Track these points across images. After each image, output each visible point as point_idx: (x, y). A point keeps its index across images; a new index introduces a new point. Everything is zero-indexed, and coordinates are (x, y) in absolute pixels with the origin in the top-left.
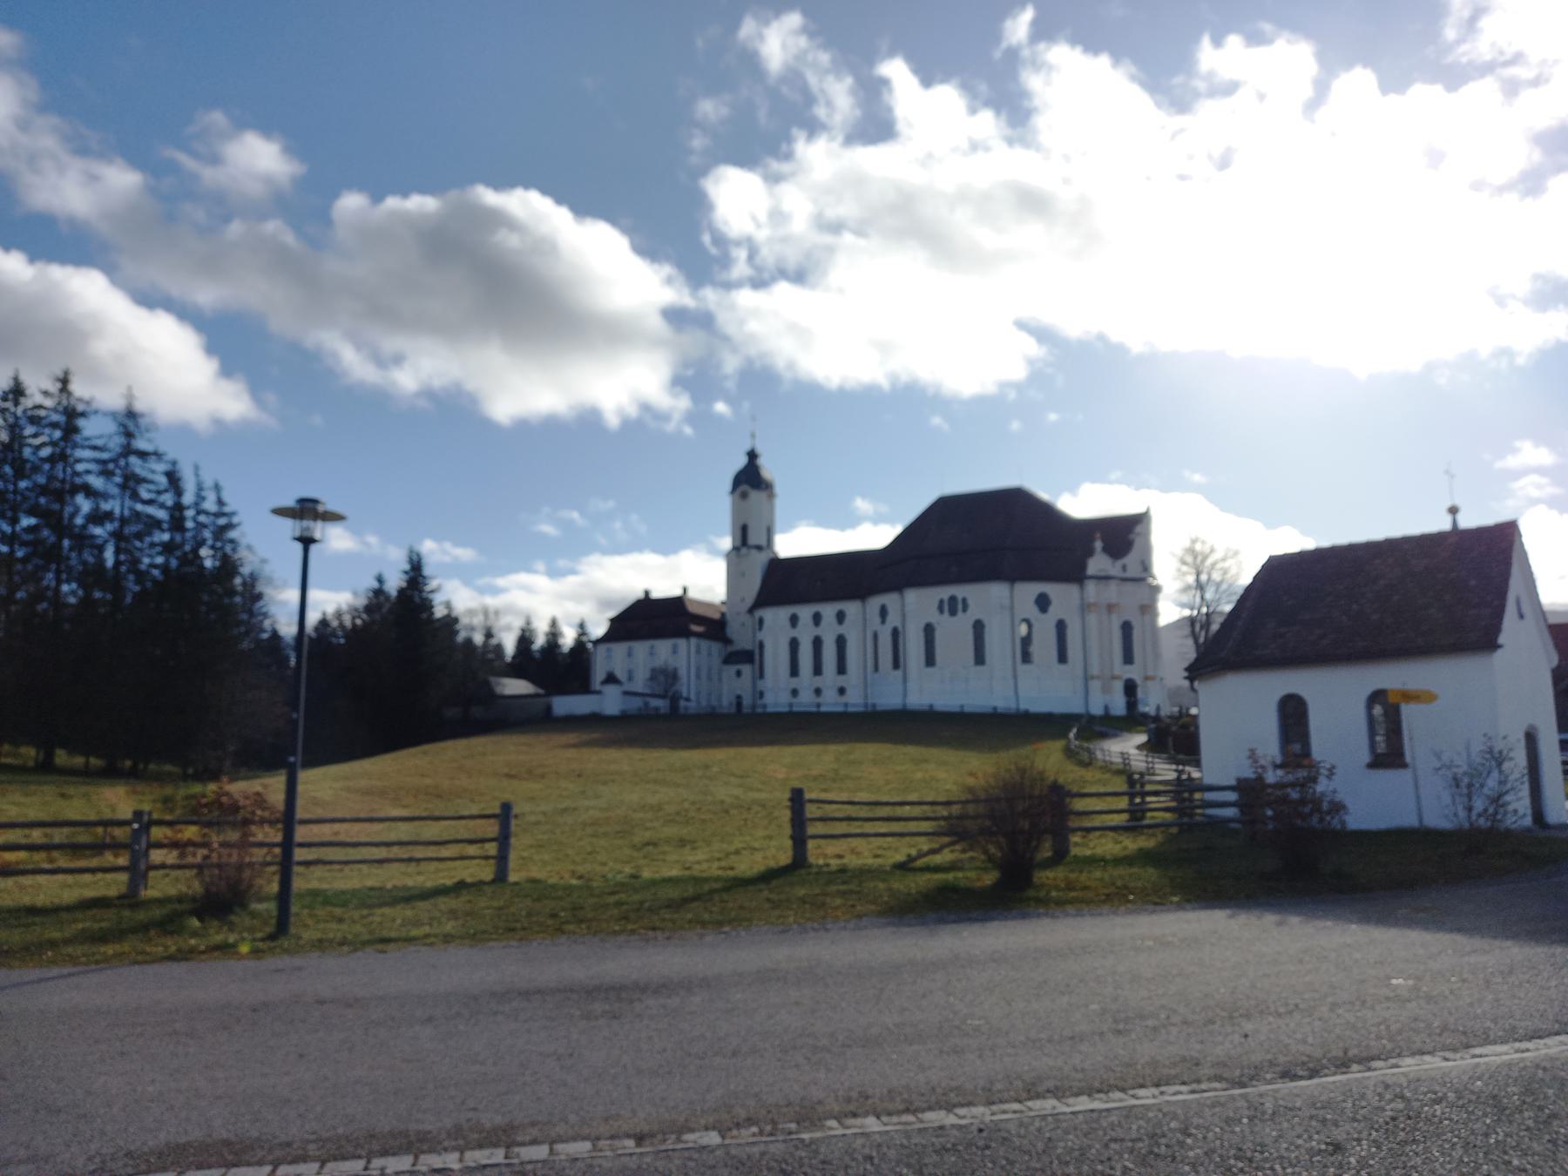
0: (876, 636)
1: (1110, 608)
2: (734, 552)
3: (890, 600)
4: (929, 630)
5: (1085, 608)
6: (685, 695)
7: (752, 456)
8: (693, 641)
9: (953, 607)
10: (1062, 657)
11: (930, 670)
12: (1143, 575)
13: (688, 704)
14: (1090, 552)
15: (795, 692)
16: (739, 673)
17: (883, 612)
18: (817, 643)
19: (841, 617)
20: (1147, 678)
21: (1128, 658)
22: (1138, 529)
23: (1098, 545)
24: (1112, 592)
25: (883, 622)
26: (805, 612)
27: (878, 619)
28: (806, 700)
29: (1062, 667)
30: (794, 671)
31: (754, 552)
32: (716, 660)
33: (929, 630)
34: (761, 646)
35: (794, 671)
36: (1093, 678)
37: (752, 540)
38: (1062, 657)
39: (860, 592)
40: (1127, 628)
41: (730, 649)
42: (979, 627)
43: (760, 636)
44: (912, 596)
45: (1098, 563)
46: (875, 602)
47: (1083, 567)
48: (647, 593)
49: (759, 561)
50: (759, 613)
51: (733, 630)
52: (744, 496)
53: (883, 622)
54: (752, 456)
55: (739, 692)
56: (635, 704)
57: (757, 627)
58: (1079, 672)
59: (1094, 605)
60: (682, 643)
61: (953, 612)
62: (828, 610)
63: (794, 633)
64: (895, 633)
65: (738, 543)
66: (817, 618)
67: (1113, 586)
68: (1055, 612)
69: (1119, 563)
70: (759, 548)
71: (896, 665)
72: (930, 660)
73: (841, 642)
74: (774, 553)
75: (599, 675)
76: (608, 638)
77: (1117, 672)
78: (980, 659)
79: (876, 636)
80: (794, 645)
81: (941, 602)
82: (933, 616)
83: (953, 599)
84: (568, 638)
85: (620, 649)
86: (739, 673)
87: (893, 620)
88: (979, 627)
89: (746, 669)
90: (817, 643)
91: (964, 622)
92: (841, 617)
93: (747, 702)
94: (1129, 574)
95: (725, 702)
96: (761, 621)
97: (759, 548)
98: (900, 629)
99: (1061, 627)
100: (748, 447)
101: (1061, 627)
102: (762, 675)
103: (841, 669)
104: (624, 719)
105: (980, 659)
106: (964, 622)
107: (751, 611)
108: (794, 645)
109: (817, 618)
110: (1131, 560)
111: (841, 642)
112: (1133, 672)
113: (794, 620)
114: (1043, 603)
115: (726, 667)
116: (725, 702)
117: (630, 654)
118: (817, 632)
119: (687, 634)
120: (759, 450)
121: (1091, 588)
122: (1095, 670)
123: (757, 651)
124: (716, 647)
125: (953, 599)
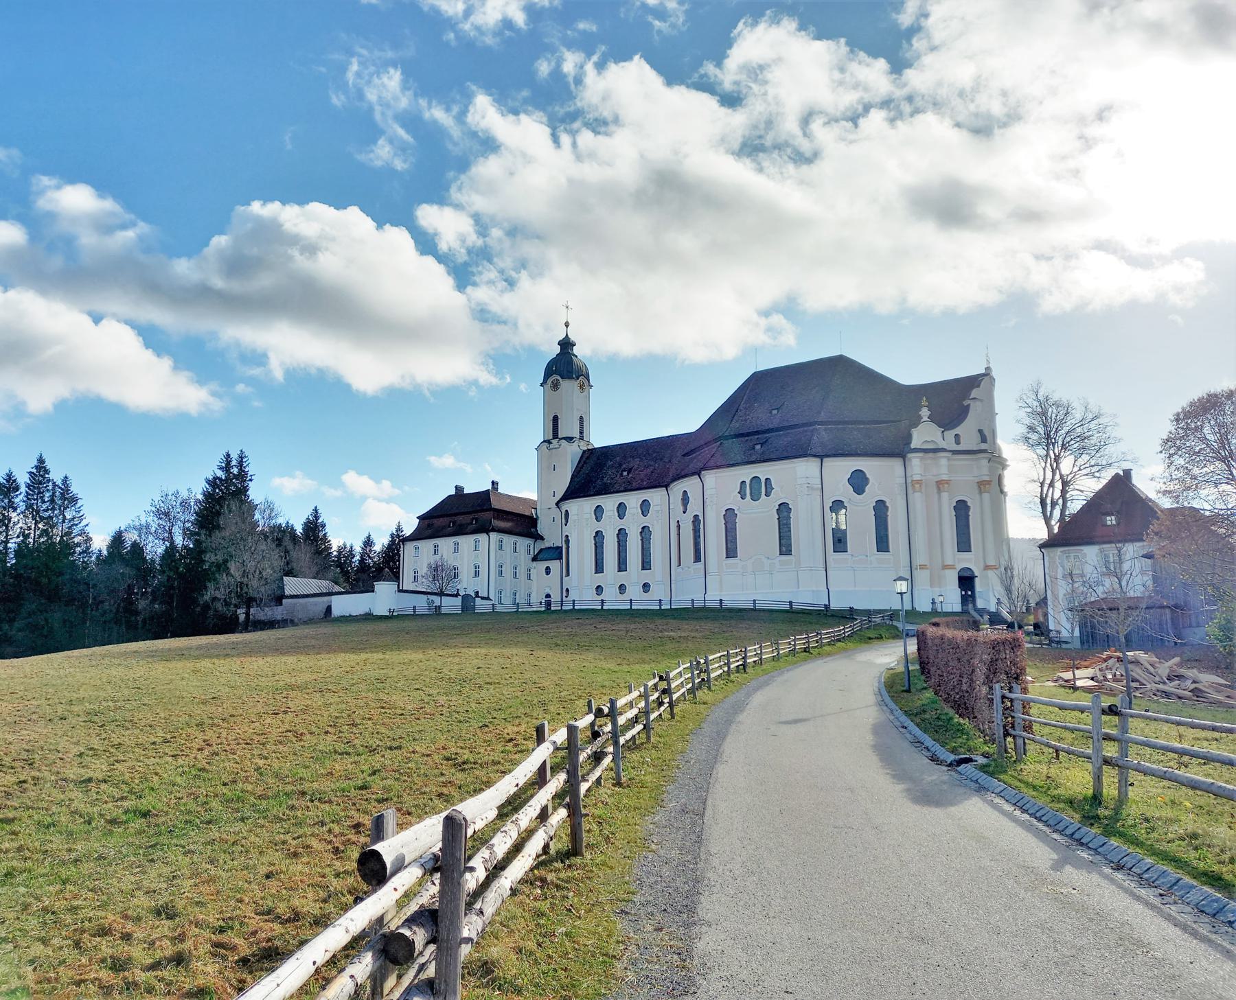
0: (679, 527)
4: (730, 516)
7: (566, 345)
8: (493, 535)
9: (756, 489)
10: (882, 544)
11: (731, 561)
14: (916, 422)
15: (599, 589)
16: (548, 571)
17: (685, 499)
18: (622, 535)
19: (645, 507)
21: (964, 544)
22: (974, 393)
23: (925, 413)
24: (942, 467)
26: (609, 503)
27: (681, 509)
28: (613, 599)
29: (883, 555)
30: (599, 568)
31: (564, 442)
32: (524, 559)
33: (730, 516)
34: (567, 541)
35: (599, 568)
38: (882, 544)
39: (661, 482)
40: (962, 509)
41: (541, 545)
42: (784, 510)
44: (710, 477)
45: (924, 434)
46: (678, 488)
47: (908, 438)
48: (459, 489)
49: (569, 457)
50: (567, 505)
51: (542, 528)
52: (555, 386)
54: (566, 345)
55: (548, 591)
59: (918, 482)
61: (755, 497)
62: (633, 500)
63: (598, 526)
66: (621, 510)
67: (943, 461)
68: (873, 492)
69: (950, 435)
70: (569, 439)
71: (697, 558)
72: (731, 552)
74: (588, 443)
77: (949, 562)
78: (785, 548)
79: (679, 527)
82: (733, 501)
83: (755, 479)
85: (426, 546)
86: (548, 571)
87: (694, 508)
88: (784, 510)
89: (555, 565)
90: (622, 535)
92: (645, 507)
93: (556, 598)
95: (535, 599)
97: (569, 439)
98: (701, 518)
99: (881, 509)
101: (881, 509)
102: (568, 574)
103: (646, 565)
105: (785, 548)
106: (766, 508)
107: (557, 504)
109: (621, 510)
110: (967, 431)
113: (599, 512)
114: (858, 482)
116: (535, 599)
120: (572, 337)
121: (915, 461)
124: (523, 543)
125: (755, 479)
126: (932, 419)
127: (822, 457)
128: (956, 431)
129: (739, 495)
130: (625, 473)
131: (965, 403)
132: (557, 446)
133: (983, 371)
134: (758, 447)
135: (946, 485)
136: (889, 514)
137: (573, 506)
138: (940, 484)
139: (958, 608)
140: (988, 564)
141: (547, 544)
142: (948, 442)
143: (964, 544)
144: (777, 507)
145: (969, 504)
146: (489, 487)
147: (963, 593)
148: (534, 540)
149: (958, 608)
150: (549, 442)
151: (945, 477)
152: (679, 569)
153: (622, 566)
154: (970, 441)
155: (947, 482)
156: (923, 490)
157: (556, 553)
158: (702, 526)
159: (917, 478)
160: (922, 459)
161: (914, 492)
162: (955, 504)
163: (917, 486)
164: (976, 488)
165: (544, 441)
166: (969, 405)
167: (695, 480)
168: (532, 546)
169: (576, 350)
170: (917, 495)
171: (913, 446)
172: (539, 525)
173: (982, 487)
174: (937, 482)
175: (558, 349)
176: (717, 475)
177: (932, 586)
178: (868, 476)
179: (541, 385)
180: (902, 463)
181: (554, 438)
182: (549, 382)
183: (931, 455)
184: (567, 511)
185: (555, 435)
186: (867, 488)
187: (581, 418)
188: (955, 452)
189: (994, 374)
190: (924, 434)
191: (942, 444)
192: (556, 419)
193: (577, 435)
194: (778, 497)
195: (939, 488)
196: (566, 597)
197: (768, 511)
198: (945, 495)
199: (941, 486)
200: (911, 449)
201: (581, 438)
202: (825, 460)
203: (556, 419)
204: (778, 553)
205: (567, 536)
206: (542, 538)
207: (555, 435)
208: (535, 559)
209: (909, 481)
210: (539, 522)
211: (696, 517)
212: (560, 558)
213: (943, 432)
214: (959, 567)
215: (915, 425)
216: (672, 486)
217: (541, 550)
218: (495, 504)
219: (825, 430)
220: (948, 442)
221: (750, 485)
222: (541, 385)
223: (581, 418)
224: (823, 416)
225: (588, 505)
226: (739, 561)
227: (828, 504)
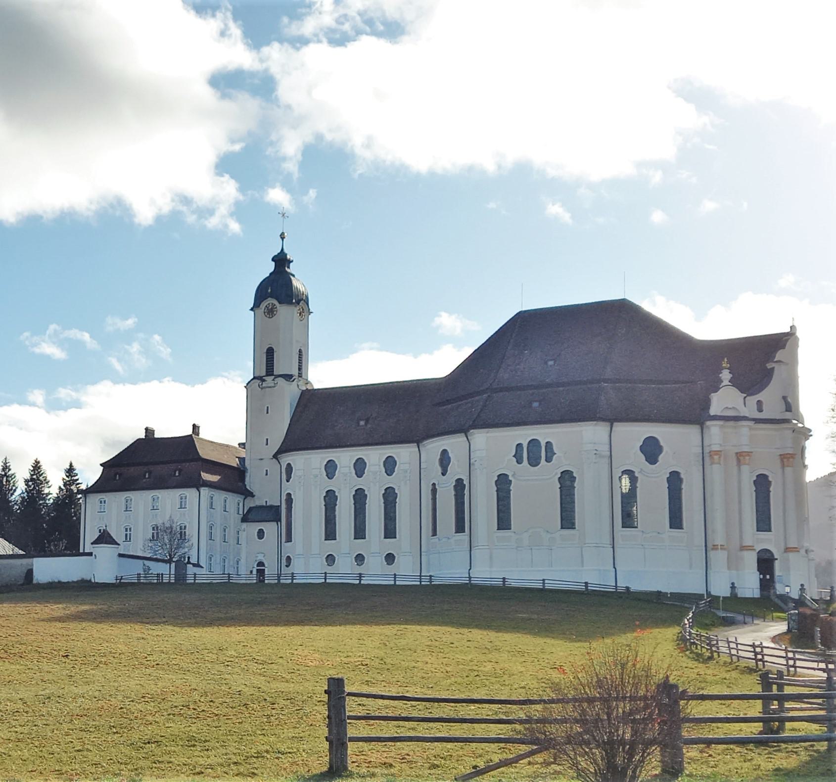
0: (434, 491)
1: (740, 457)
3: (453, 444)
4: (503, 482)
5: (706, 457)
6: (194, 560)
7: (281, 261)
12: (788, 415)
13: (197, 570)
16: (261, 534)
17: (444, 460)
18: (360, 497)
19: (390, 465)
20: (787, 550)
21: (764, 523)
22: (779, 356)
24: (744, 435)
25: (443, 474)
26: (345, 458)
27: (439, 470)
30: (330, 534)
31: (280, 381)
33: (503, 482)
34: (289, 499)
35: (330, 534)
36: (715, 547)
37: (280, 368)
40: (762, 484)
41: (251, 503)
42: (567, 480)
43: (288, 488)
44: (481, 438)
46: (434, 447)
50: (287, 459)
51: (252, 481)
53: (443, 474)
54: (281, 261)
56: (132, 571)
59: (717, 453)
60: (190, 494)
61: (534, 461)
62: (374, 456)
63: (331, 485)
64: (459, 486)
66: (360, 467)
67: (745, 428)
70: (288, 377)
71: (460, 528)
73: (390, 497)
75: (89, 533)
76: (99, 487)
79: (434, 491)
80: (330, 499)
81: (519, 446)
84: (54, 486)
86: (261, 534)
87: (457, 470)
88: (567, 480)
90: (360, 497)
92: (390, 465)
93: (270, 571)
95: (243, 571)
96: (289, 469)
97: (288, 377)
98: (466, 482)
99: (675, 481)
101: (675, 481)
102: (289, 539)
103: (390, 532)
104: (119, 587)
107: (275, 456)
108: (330, 499)
109: (360, 467)
111: (390, 497)
112: (769, 541)
113: (331, 468)
115: (244, 525)
116: (243, 571)
118: (360, 483)
119: (198, 484)
121: (714, 429)
122: (719, 538)
123: (284, 506)
125: (534, 443)
126: (734, 382)
129: (515, 459)
130: (362, 423)
132: (273, 385)
134: (535, 404)
135: (747, 458)
136: (683, 486)
137: (298, 460)
138: (739, 456)
139: (757, 594)
140: (789, 546)
141: (259, 501)
142: (747, 407)
143: (764, 523)
145: (770, 479)
147: (762, 576)
148: (243, 497)
149: (757, 594)
150: (261, 379)
151: (746, 449)
152: (435, 540)
153: (360, 532)
154: (773, 409)
155: (749, 454)
156: (722, 462)
157: (271, 513)
158: (466, 492)
159: (715, 448)
160: (721, 427)
161: (712, 463)
162: (755, 478)
163: (716, 457)
164: (779, 461)
165: (254, 378)
166: (773, 368)
168: (241, 504)
169: (292, 269)
170: (715, 466)
171: (713, 411)
172: (247, 479)
173: (785, 460)
174: (737, 453)
175: (271, 267)
176: (488, 435)
177: (729, 568)
178: (662, 443)
180: (700, 430)
181: (267, 375)
182: (263, 305)
184: (289, 465)
185: (270, 371)
186: (660, 458)
187: (300, 351)
189: (799, 334)
191: (744, 412)
192: (270, 352)
193: (295, 372)
195: (739, 461)
196: (287, 566)
197: (551, 478)
198: (745, 469)
199: (741, 458)
200: (710, 416)
201: (300, 375)
202: (615, 424)
203: (270, 352)
204: (560, 527)
205: (289, 495)
206: (251, 495)
207: (270, 371)
208: (245, 519)
209: (707, 450)
210: (248, 475)
211: (459, 482)
212: (278, 520)
213: (745, 398)
214: (758, 548)
215: (716, 389)
217: (251, 509)
218: (204, 453)
220: (749, 410)
221: (528, 448)
222: (252, 309)
223: (300, 351)
224: (609, 373)
225: (316, 460)
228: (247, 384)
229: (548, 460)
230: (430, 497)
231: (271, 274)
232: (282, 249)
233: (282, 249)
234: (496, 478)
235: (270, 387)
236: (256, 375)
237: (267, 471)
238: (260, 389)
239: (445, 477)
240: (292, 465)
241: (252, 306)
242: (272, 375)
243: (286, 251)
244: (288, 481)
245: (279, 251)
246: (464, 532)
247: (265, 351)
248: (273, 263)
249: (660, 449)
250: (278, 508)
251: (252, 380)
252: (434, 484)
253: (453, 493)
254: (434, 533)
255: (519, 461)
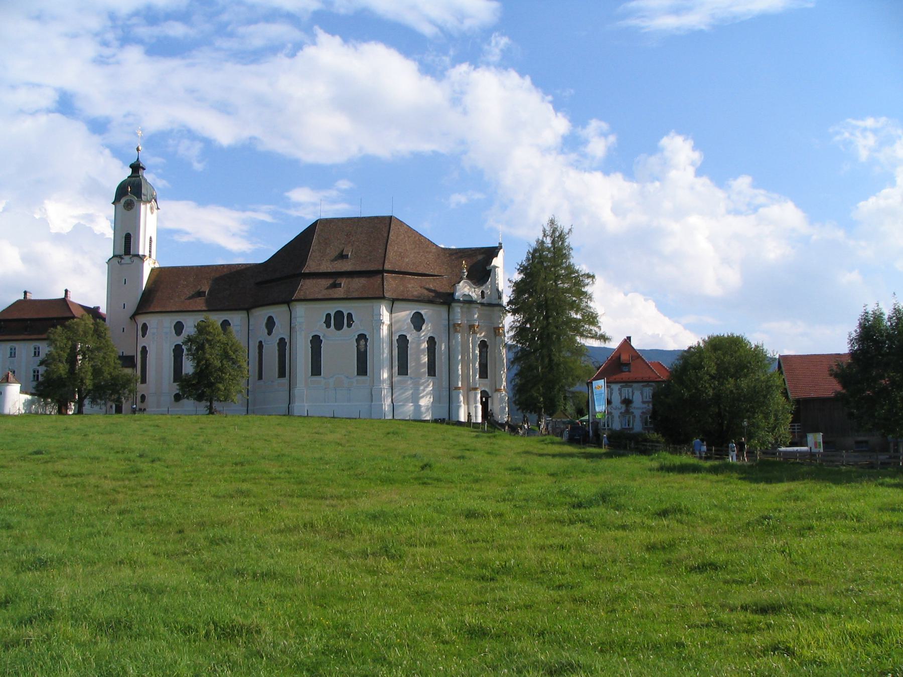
2: (116, 260)
3: (278, 312)
4: (316, 342)
5: (452, 328)
9: (339, 321)
17: (270, 324)
25: (270, 333)
27: (266, 331)
31: (136, 259)
33: (316, 342)
34: (144, 349)
43: (142, 342)
44: (300, 310)
46: (261, 315)
50: (141, 320)
52: (129, 206)
53: (270, 333)
57: (140, 333)
58: (445, 384)
61: (338, 326)
65: (121, 251)
68: (427, 330)
71: (282, 374)
72: (316, 370)
78: (362, 369)
81: (328, 315)
82: (320, 329)
83: (339, 314)
87: (280, 330)
91: (348, 336)
94: (485, 301)
96: (145, 328)
99: (432, 341)
100: (134, 160)
102: (144, 381)
105: (362, 369)
106: (348, 336)
107: (133, 317)
113: (179, 328)
114: (418, 321)
117: (13, 355)
120: (143, 163)
121: (457, 309)
125: (339, 314)
127: (393, 301)
128: (483, 288)
129: (325, 325)
131: (488, 268)
132: (130, 262)
133: (497, 245)
137: (151, 320)
144: (356, 337)
146: (63, 296)
150: (120, 257)
152: (261, 382)
158: (287, 347)
159: (460, 323)
160: (461, 308)
165: (114, 256)
167: (284, 308)
179: (113, 203)
182: (123, 201)
183: (467, 305)
188: (482, 304)
190: (465, 289)
193: (147, 254)
194: (358, 327)
202: (397, 304)
209: (451, 323)
212: (134, 366)
216: (253, 311)
219: (392, 277)
222: (113, 203)
225: (169, 322)
226: (322, 379)
227: (396, 338)
228: (109, 261)
229: (349, 325)
230: (257, 351)
231: (128, 177)
232: (138, 159)
233: (138, 159)
234: (311, 338)
235: (128, 264)
236: (117, 253)
237: (124, 329)
238: (119, 265)
239: (270, 337)
240: (148, 325)
241: (113, 200)
242: (130, 254)
243: (140, 159)
244: (143, 336)
245: (135, 160)
246: (285, 377)
247: (124, 235)
248: (131, 170)
249: (423, 321)
250: (134, 356)
251: (113, 257)
252: (261, 342)
253: (277, 348)
254: (260, 377)
255: (328, 326)
